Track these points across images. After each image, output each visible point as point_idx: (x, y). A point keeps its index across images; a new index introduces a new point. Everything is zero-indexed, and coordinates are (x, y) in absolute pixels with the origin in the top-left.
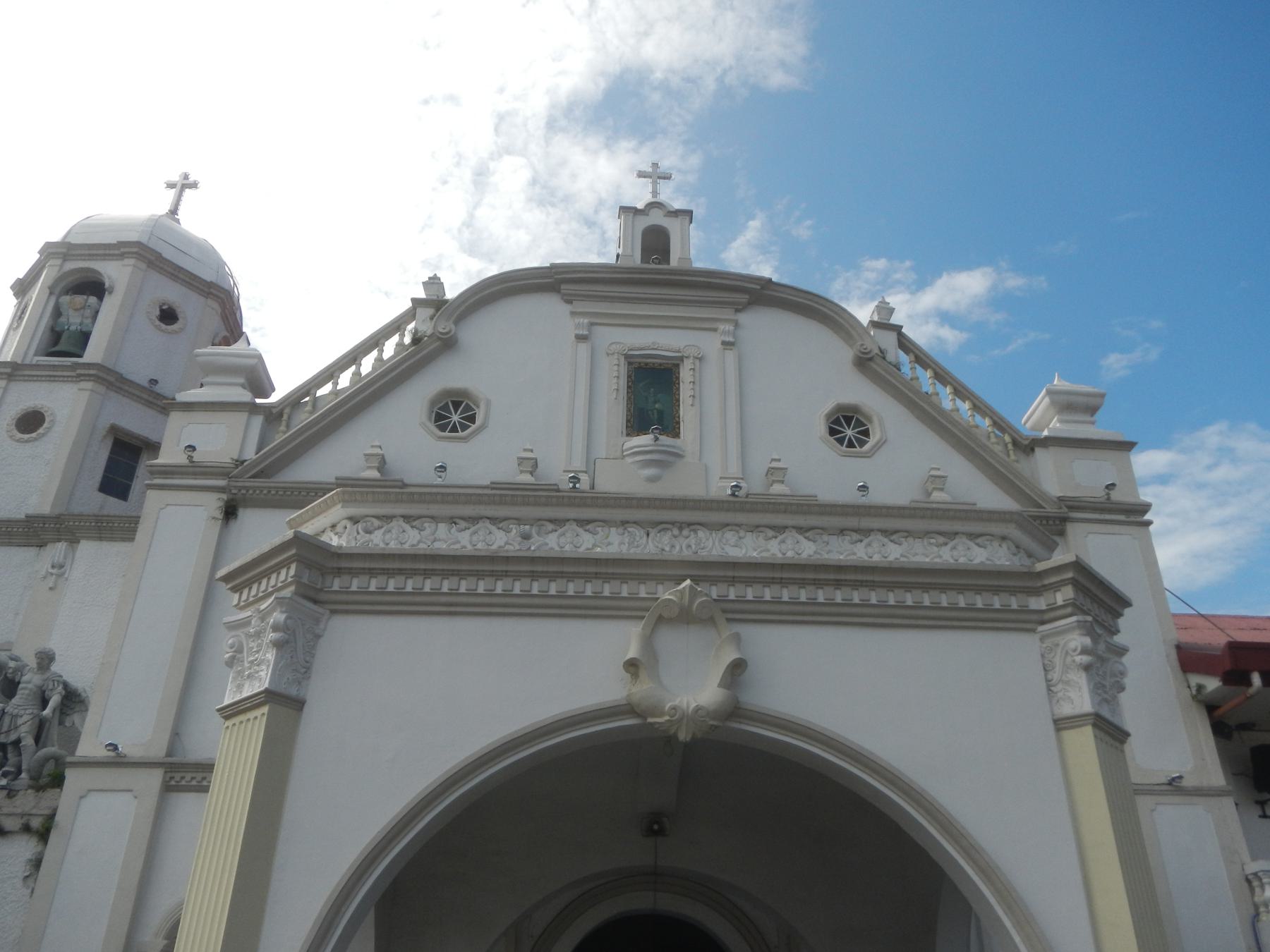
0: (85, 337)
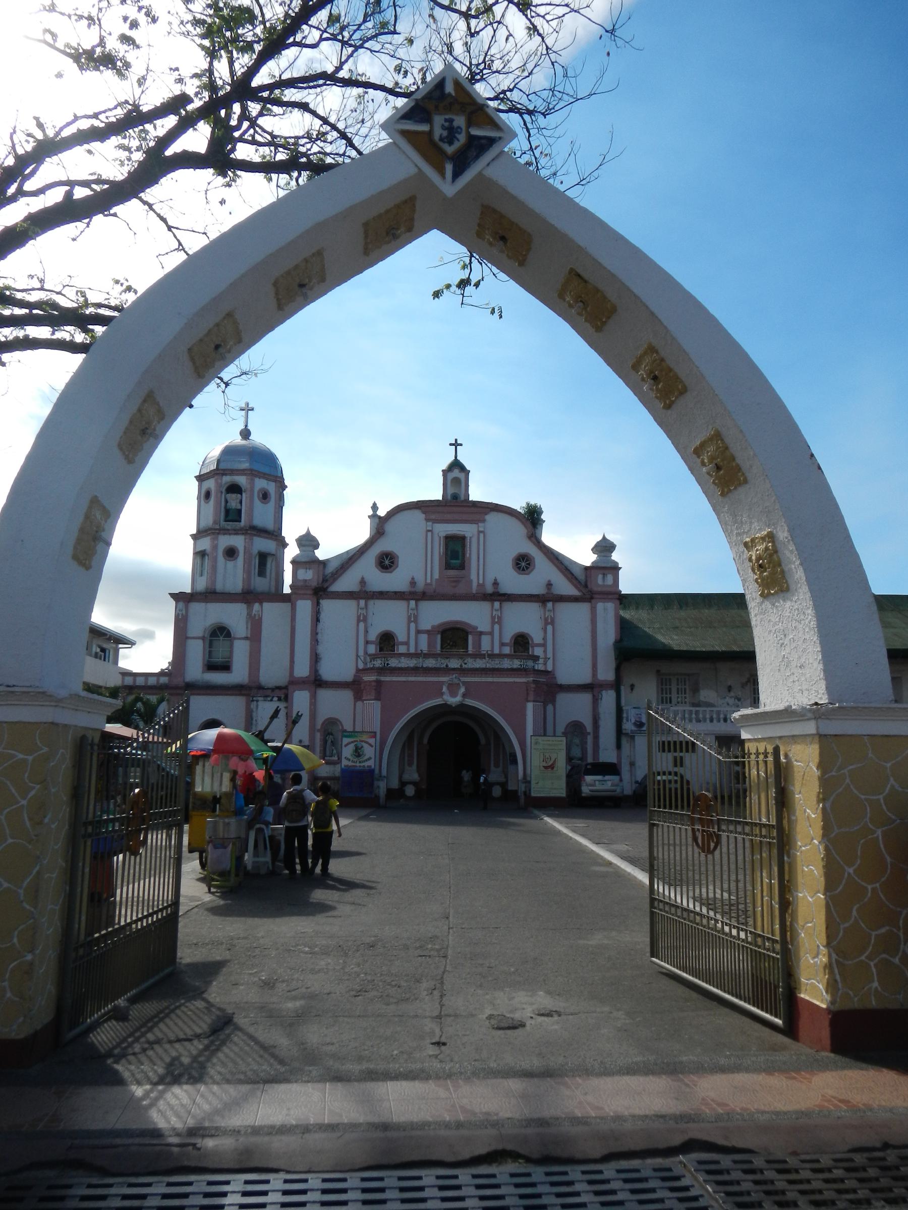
0: (240, 511)
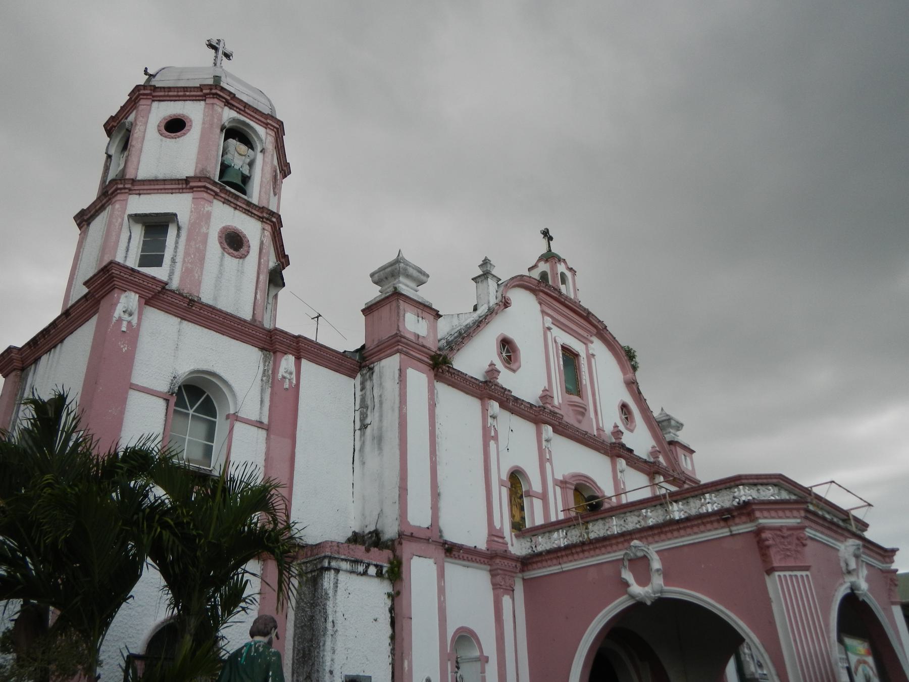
0: (246, 179)
